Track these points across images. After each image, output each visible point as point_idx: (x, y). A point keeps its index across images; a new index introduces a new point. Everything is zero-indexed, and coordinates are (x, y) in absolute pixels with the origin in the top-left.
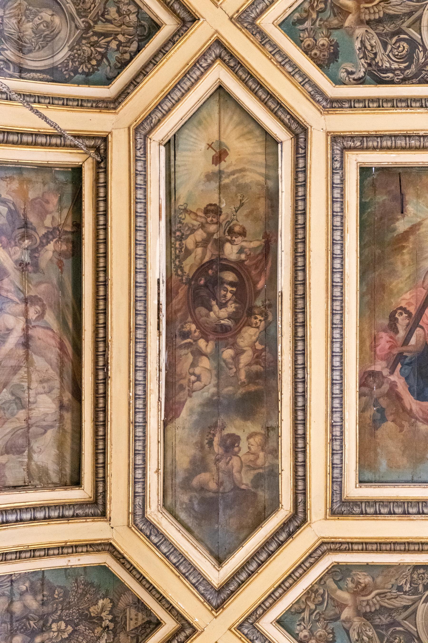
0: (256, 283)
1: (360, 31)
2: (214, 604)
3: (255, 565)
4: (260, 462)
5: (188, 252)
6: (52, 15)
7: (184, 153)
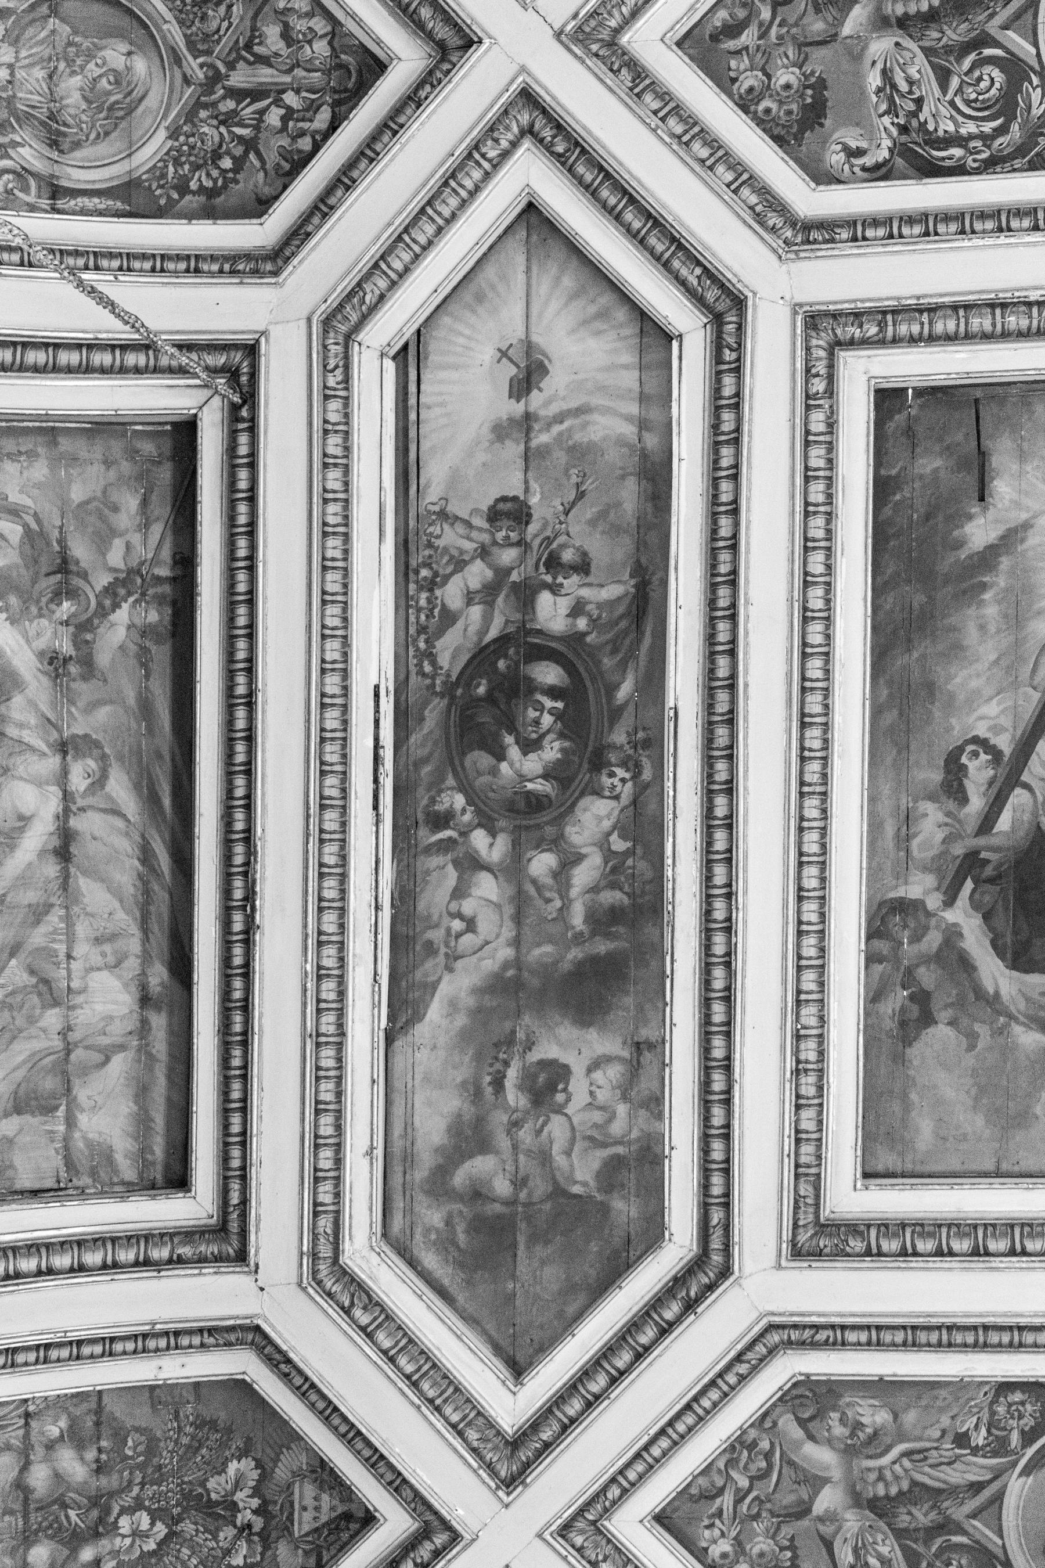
0: (612, 689)
1: (880, 46)
2: (503, 1474)
3: (602, 1380)
4: (617, 1128)
5: (449, 618)
6: (129, 54)
7: (443, 375)
